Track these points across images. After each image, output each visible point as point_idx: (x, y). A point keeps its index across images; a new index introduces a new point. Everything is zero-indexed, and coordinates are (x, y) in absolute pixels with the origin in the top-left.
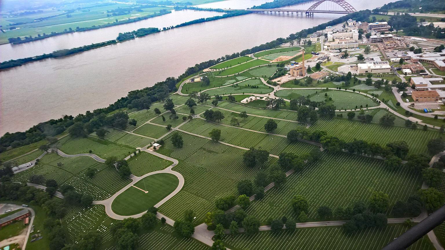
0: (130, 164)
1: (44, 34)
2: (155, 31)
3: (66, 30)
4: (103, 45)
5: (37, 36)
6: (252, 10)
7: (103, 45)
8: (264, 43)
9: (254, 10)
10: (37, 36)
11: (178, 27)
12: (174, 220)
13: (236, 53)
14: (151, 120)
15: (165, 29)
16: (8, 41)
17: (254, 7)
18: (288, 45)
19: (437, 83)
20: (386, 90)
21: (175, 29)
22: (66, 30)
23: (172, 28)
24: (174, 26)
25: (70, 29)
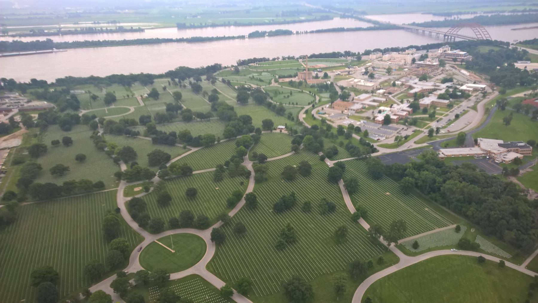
0: (290, 149)
1: (206, 24)
2: (288, 33)
3: (225, 23)
4: (233, 38)
5: (199, 25)
6: (409, 27)
7: (233, 38)
8: (323, 52)
9: (411, 27)
10: (199, 25)
11: (312, 32)
12: (234, 217)
13: (267, 57)
14: (127, 113)
15: (297, 33)
16: (176, 25)
17: (414, 24)
18: (343, 58)
19: (361, 229)
20: (288, 180)
21: (309, 35)
22: (225, 23)
23: (306, 33)
24: (308, 31)
25: (229, 22)
